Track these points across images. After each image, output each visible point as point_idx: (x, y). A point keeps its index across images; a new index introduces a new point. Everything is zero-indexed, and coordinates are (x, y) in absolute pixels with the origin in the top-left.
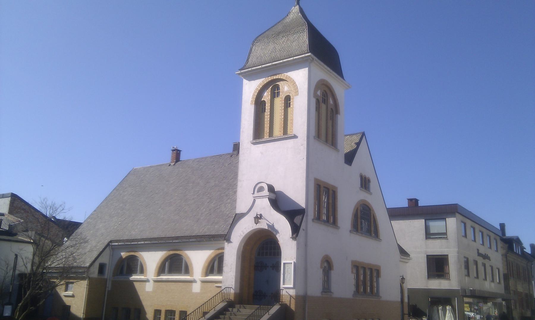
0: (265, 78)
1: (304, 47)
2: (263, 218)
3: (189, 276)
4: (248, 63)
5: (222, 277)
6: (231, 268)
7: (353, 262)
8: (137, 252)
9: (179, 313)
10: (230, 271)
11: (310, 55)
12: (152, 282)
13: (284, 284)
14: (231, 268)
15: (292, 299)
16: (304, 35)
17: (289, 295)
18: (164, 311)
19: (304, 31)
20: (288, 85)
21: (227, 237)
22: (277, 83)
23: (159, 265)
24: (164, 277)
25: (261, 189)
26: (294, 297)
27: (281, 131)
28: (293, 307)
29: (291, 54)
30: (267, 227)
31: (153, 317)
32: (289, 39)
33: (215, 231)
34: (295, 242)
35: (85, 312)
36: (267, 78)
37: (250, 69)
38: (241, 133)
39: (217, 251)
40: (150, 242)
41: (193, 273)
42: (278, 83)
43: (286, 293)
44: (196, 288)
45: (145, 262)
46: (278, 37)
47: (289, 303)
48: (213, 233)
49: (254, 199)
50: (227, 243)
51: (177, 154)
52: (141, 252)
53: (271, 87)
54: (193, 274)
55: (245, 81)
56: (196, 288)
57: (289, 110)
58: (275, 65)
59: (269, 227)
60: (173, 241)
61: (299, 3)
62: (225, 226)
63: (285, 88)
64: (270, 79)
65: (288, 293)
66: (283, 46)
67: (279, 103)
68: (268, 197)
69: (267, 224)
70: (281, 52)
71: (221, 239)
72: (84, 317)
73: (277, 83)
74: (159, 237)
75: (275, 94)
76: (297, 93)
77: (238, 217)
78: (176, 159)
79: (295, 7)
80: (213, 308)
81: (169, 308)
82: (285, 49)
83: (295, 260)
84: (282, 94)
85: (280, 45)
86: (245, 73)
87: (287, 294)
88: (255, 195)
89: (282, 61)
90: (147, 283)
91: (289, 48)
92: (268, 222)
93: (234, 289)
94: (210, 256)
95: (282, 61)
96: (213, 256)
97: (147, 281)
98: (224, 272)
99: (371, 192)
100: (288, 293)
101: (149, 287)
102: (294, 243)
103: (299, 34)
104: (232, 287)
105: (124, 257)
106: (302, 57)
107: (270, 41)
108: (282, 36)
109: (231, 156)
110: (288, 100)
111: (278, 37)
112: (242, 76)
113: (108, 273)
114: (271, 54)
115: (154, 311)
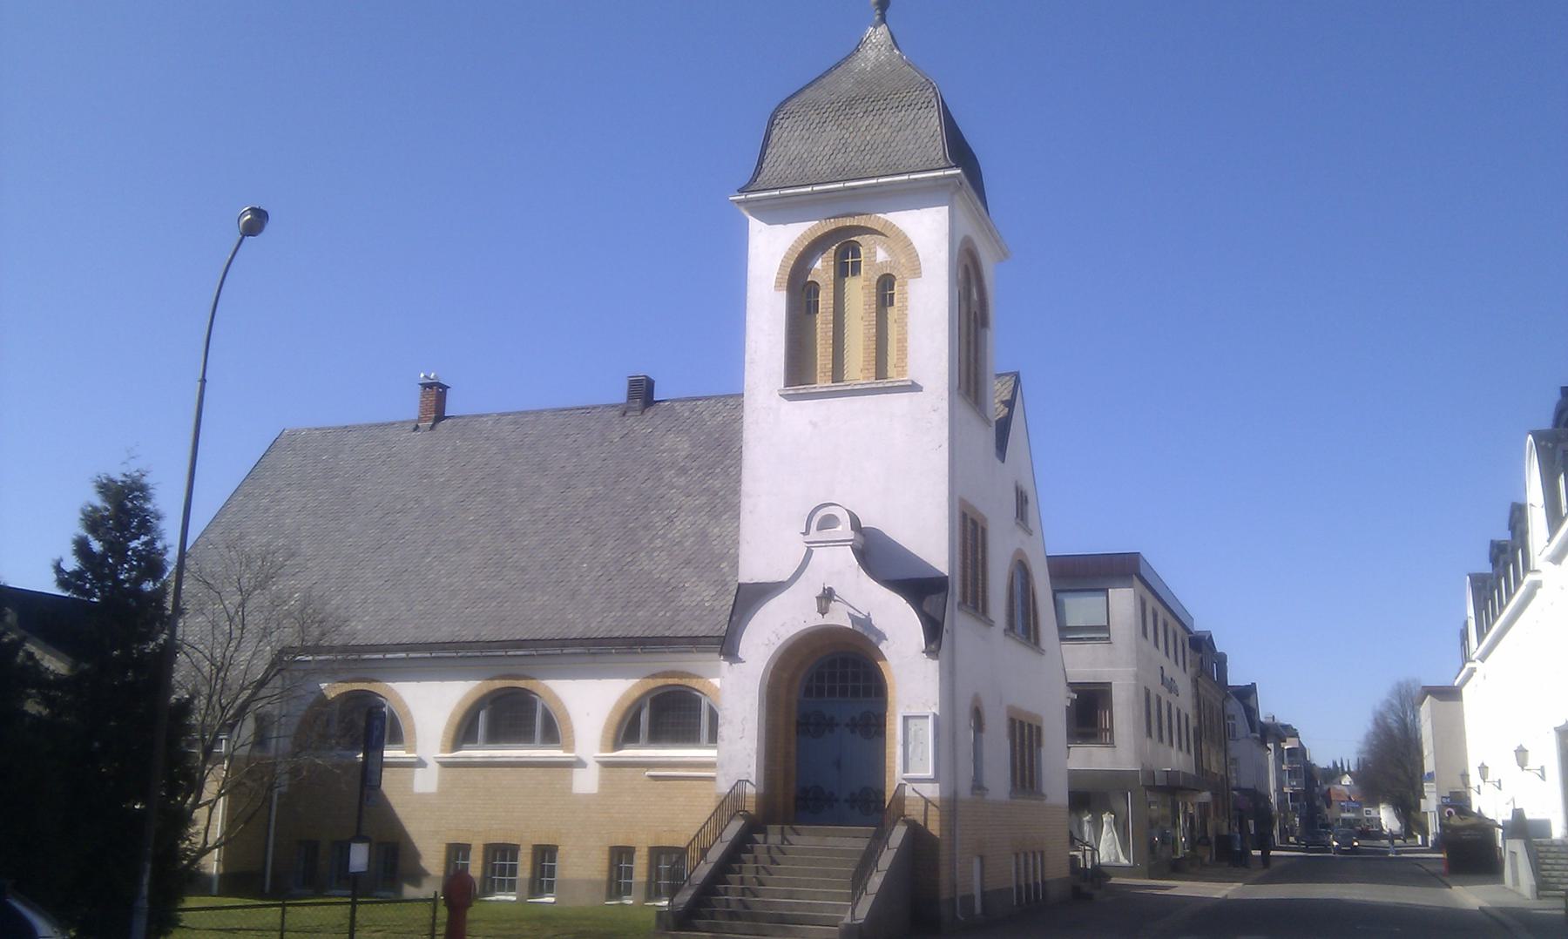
0: (817, 222)
1: (933, 148)
2: (836, 598)
3: (560, 748)
4: (762, 175)
5: (716, 751)
6: (744, 729)
7: (1011, 709)
8: (377, 681)
9: (530, 851)
10: (741, 738)
11: (958, 174)
12: (433, 770)
13: (906, 769)
14: (744, 729)
15: (931, 807)
16: (930, 115)
17: (922, 796)
18: (646, 849)
19: (930, 105)
20: (888, 246)
21: (727, 645)
22: (852, 239)
23: (458, 718)
24: (629, 753)
25: (828, 522)
26: (938, 804)
27: (868, 369)
28: (934, 827)
29: (897, 163)
30: (850, 621)
31: (443, 865)
32: (885, 121)
33: (643, 626)
34: (936, 663)
35: (224, 856)
36: (824, 221)
37: (777, 193)
38: (747, 365)
39: (650, 680)
40: (428, 655)
41: (574, 741)
42: (855, 239)
43: (912, 791)
44: (586, 782)
45: (408, 710)
46: (851, 112)
47: (923, 818)
48: (638, 632)
49: (808, 547)
50: (727, 663)
51: (436, 392)
52: (393, 682)
53: (834, 248)
54: (574, 745)
55: (755, 225)
56: (586, 782)
57: (892, 313)
58: (853, 188)
59: (857, 624)
60: (506, 652)
61: (885, 16)
62: (668, 614)
63: (877, 255)
64: (832, 225)
65: (919, 793)
66: (868, 138)
67: (859, 292)
68: (851, 543)
69: (849, 614)
70: (864, 153)
71: (667, 650)
72: (221, 871)
73: (852, 239)
74: (456, 639)
75: (847, 265)
76: (916, 271)
77: (752, 597)
78: (436, 412)
79: (875, 27)
80: (717, 839)
81: (545, 842)
82: (875, 147)
83: (936, 710)
84: (870, 269)
85: (860, 134)
86: (758, 200)
87: (918, 795)
88: (808, 538)
89: (874, 181)
90: (418, 771)
91: (887, 145)
92: (855, 609)
93: (754, 783)
94: (624, 697)
95: (874, 181)
96: (637, 694)
97: (420, 763)
98: (723, 740)
99: (1030, 526)
100: (919, 793)
101: (426, 781)
102: (932, 667)
103: (916, 110)
104: (750, 779)
105: (331, 695)
106: (934, 177)
107: (828, 120)
108: (864, 110)
109: (624, 415)
110: (885, 288)
111: (851, 112)
112: (746, 209)
113: (280, 743)
114: (833, 157)
115: (446, 848)
